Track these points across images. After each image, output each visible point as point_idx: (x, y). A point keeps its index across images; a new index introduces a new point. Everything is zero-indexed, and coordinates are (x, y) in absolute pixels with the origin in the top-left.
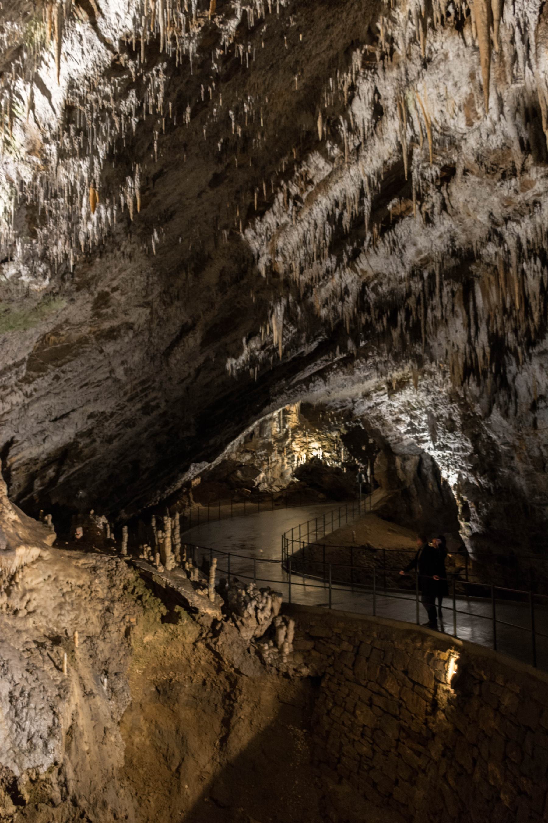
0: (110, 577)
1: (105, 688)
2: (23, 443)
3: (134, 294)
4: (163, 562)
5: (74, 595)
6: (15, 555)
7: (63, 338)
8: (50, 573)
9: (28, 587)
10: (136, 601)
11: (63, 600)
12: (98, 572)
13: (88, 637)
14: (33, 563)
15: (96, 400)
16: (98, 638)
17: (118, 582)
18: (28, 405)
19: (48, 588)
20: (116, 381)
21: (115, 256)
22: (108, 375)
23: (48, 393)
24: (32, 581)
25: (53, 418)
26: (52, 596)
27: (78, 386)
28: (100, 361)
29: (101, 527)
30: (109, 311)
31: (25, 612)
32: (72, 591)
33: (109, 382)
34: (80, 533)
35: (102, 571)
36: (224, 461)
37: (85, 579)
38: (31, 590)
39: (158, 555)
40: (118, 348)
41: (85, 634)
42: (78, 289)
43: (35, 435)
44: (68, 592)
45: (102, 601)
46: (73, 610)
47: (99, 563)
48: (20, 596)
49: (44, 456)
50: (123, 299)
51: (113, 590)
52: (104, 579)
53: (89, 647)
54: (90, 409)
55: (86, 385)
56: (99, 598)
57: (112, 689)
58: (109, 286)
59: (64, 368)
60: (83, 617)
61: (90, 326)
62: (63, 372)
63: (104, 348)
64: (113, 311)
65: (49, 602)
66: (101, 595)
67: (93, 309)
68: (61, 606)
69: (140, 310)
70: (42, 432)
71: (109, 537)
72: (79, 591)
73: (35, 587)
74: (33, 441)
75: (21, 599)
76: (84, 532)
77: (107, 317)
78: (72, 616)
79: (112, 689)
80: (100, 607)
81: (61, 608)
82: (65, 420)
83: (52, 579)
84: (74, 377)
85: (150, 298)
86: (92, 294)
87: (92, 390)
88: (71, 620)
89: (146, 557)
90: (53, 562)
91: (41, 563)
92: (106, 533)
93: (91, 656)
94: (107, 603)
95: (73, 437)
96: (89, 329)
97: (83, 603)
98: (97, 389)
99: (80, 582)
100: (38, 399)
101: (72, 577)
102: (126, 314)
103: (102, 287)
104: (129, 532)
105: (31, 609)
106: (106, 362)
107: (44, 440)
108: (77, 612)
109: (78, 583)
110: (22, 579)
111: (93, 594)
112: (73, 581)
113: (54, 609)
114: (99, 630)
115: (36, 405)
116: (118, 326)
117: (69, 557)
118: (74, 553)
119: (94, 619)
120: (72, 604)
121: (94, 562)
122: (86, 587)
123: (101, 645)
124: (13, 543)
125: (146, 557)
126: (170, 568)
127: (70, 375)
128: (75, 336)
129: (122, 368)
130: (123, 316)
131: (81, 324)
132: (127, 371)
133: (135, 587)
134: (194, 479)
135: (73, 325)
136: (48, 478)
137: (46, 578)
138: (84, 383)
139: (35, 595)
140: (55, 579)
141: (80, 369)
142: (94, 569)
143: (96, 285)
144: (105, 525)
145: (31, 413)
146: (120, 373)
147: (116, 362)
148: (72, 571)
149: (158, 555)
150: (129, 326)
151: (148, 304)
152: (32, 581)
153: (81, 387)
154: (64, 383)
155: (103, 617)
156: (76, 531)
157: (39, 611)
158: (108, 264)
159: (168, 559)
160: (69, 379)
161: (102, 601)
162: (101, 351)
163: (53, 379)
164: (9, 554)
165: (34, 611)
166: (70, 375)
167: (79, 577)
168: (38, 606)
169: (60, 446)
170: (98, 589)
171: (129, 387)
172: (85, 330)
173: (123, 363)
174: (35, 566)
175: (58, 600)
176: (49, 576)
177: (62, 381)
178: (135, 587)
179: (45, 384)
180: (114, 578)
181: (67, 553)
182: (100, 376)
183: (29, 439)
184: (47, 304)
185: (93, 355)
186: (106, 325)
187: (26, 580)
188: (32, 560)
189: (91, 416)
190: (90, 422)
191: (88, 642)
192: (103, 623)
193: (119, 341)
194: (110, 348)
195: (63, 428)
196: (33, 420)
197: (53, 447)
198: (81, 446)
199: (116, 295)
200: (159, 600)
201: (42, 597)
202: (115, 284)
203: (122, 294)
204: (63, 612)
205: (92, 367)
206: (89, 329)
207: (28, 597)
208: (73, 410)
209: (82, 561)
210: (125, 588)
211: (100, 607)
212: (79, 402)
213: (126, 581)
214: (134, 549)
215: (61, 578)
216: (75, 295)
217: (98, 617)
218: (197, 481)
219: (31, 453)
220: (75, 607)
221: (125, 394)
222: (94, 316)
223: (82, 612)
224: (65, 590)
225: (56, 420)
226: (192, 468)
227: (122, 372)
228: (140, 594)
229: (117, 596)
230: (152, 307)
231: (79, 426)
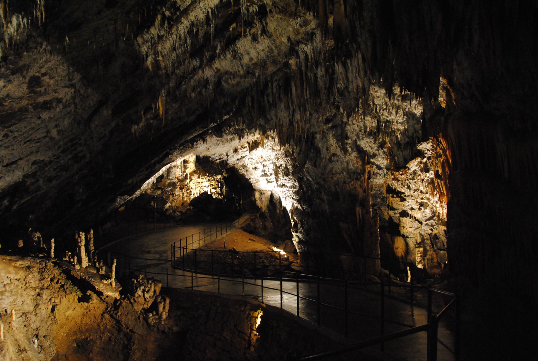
0: (41, 272)
1: (36, 346)
3: (60, 79)
4: (80, 261)
7: (7, 108)
10: (60, 289)
11: (4, 289)
12: (31, 269)
13: (23, 313)
15: (37, 152)
16: (31, 314)
17: (47, 276)
20: (52, 138)
21: (39, 52)
22: (45, 134)
25: (5, 164)
27: (23, 142)
28: (39, 124)
29: (36, 239)
30: (42, 89)
32: (11, 283)
33: (47, 139)
34: (21, 244)
35: (34, 269)
36: (141, 195)
37: (21, 274)
39: (76, 258)
40: (52, 115)
41: (21, 311)
42: (13, 73)
44: (8, 284)
45: (35, 289)
46: (12, 295)
47: (32, 264)
50: (52, 82)
51: (43, 281)
52: (36, 274)
53: (24, 319)
54: (33, 158)
55: (29, 141)
57: (41, 346)
58: (38, 72)
59: (11, 128)
60: (20, 300)
61: (28, 100)
62: (11, 131)
63: (41, 115)
64: (45, 89)
66: (33, 285)
67: (28, 87)
69: (66, 90)
71: (42, 246)
72: (17, 283)
76: (24, 243)
77: (40, 94)
78: (11, 299)
79: (41, 346)
80: (33, 293)
82: (14, 166)
84: (20, 135)
85: (74, 81)
86: (24, 77)
87: (34, 145)
88: (11, 302)
89: (67, 259)
92: (40, 244)
93: (25, 326)
94: (38, 291)
95: (21, 178)
96: (27, 102)
97: (20, 291)
98: (38, 144)
99: (18, 277)
102: (56, 92)
103: (32, 73)
104: (55, 243)
106: (43, 125)
108: (15, 297)
109: (16, 278)
111: (27, 285)
112: (12, 276)
114: (32, 308)
116: (50, 101)
117: (9, 260)
118: (13, 258)
119: (29, 301)
121: (29, 263)
122: (22, 280)
123: (33, 318)
125: (67, 259)
126: (84, 267)
127: (16, 134)
128: (16, 106)
129: (56, 130)
130: (54, 93)
131: (21, 98)
132: (59, 132)
133: (59, 279)
134: (120, 207)
135: (14, 99)
136: (3, 206)
138: (27, 140)
141: (24, 130)
142: (29, 268)
143: (27, 71)
144: (39, 238)
146: (54, 133)
147: (52, 125)
148: (11, 269)
149: (76, 258)
150: (59, 101)
151: (72, 86)
153: (25, 143)
154: (12, 140)
155: (35, 299)
156: (18, 243)
158: (34, 57)
159: (83, 260)
161: (35, 289)
162: (39, 118)
163: (3, 137)
166: (16, 134)
167: (17, 273)
169: (11, 184)
170: (31, 281)
171: (61, 143)
172: (24, 103)
173: (56, 126)
177: (11, 138)
178: (59, 279)
180: (44, 274)
181: (8, 258)
182: (39, 135)
185: (33, 120)
186: (41, 99)
189: (34, 163)
190: (33, 167)
191: (24, 316)
192: (35, 304)
193: (52, 111)
194: (45, 115)
195: (13, 171)
197: (6, 184)
198: (28, 184)
199: (46, 78)
200: (76, 288)
202: (43, 71)
203: (51, 78)
204: (4, 297)
205: (33, 128)
206: (27, 102)
208: (21, 159)
209: (20, 263)
210: (52, 280)
211: (33, 293)
212: (24, 153)
213: (52, 276)
214: (60, 253)
216: (12, 77)
217: (31, 299)
218: (123, 208)
220: (13, 293)
221: (59, 148)
222: (30, 93)
223: (19, 297)
224: (5, 283)
225: (7, 165)
226: (118, 200)
227: (56, 133)
228: (63, 283)
229: (46, 286)
230: (75, 88)
231: (26, 170)
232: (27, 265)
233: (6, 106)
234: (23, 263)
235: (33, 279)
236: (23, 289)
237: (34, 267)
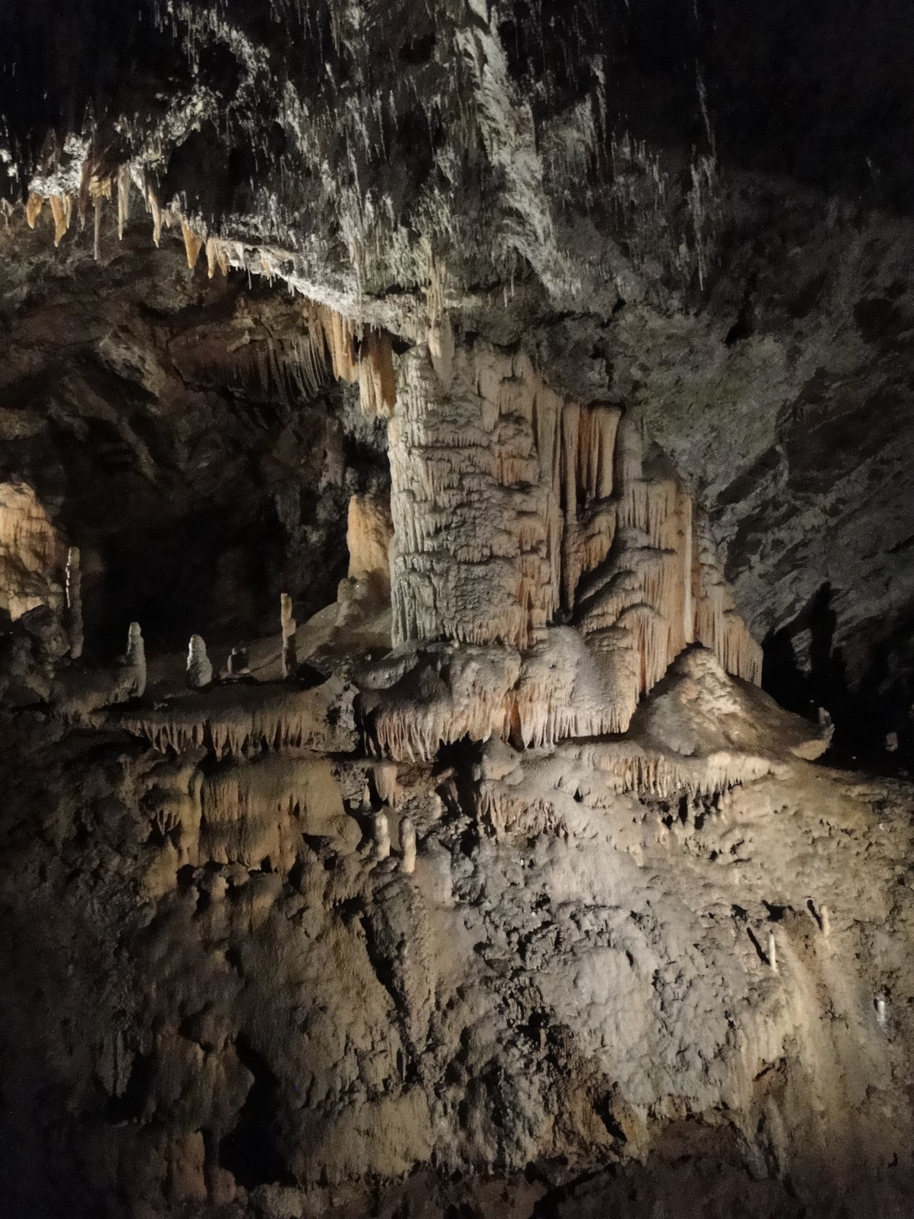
1: (882, 1019)
2: (847, 593)
5: (833, 845)
6: (706, 766)
7: (832, 405)
8: (786, 801)
9: (740, 819)
11: (810, 850)
12: (887, 811)
13: (857, 922)
14: (754, 782)
16: (879, 927)
18: (836, 528)
19: (781, 827)
23: (866, 504)
24: (748, 811)
26: (789, 840)
31: (731, 858)
32: (831, 837)
34: (892, 742)
35: (898, 811)
37: (857, 820)
38: (746, 826)
41: (852, 916)
43: (866, 579)
44: (821, 838)
45: (892, 863)
46: (830, 869)
48: (721, 830)
49: (894, 613)
53: (857, 939)
56: (884, 858)
57: (898, 1025)
58: (871, 287)
59: (881, 454)
60: (850, 887)
65: (779, 849)
66: (889, 851)
68: (803, 860)
70: (877, 572)
72: (846, 839)
73: (755, 821)
74: (864, 588)
75: (723, 836)
76: (900, 739)
78: (828, 879)
79: (898, 1025)
80: (887, 874)
81: (803, 864)
83: (792, 812)
88: (826, 886)
90: (799, 785)
91: (770, 784)
93: (858, 956)
94: (899, 869)
99: (848, 825)
100: (851, 516)
101: (831, 814)
105: (743, 853)
107: (887, 585)
108: (839, 876)
109: (843, 827)
110: (731, 806)
111: (873, 849)
112: (833, 821)
113: (789, 864)
114: (883, 914)
115: (850, 526)
117: (835, 780)
118: (848, 775)
119: (875, 892)
120: (829, 860)
121: (885, 793)
123: (882, 940)
124: (705, 747)
127: (898, 467)
128: (860, 396)
137: (779, 809)
139: (750, 834)
140: (796, 814)
142: (880, 805)
145: (843, 542)
148: (834, 803)
152: (748, 811)
155: (892, 892)
156: (885, 740)
157: (756, 861)
160: (900, 473)
161: (892, 863)
164: (697, 762)
165: (749, 860)
167: (844, 816)
168: (756, 853)
172: (878, 380)
174: (757, 787)
175: (801, 850)
176: (785, 807)
179: (859, 489)
181: (834, 774)
183: (855, 586)
184: (742, 355)
187: (737, 808)
188: (753, 777)
191: (856, 930)
192: (891, 905)
196: (851, 553)
201: (765, 838)
204: (808, 870)
207: (737, 835)
209: (857, 790)
211: (887, 874)
215: (808, 813)
216: (798, 324)
217: (881, 890)
219: (866, 609)
220: (835, 865)
222: (883, 352)
223: (849, 875)
224: (816, 834)
225: (895, 551)
232: (878, 798)
233: (830, 399)
234: (868, 792)
235: (892, 836)
236: (861, 857)
237: (895, 805)
